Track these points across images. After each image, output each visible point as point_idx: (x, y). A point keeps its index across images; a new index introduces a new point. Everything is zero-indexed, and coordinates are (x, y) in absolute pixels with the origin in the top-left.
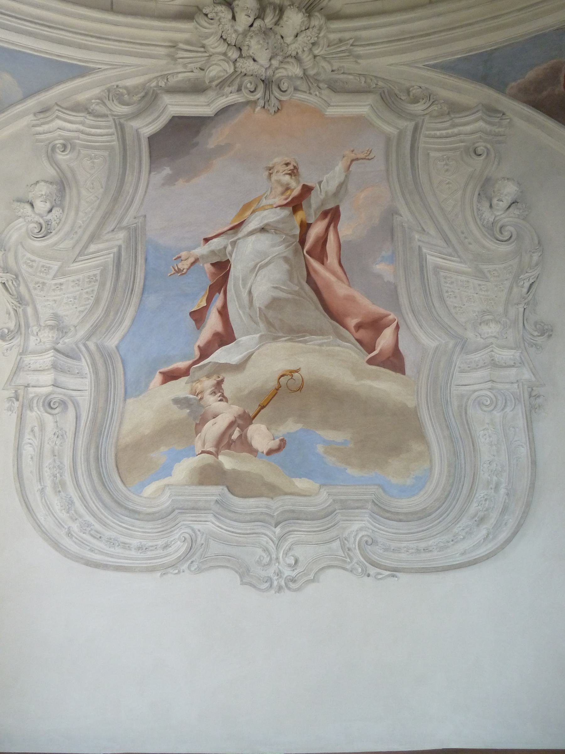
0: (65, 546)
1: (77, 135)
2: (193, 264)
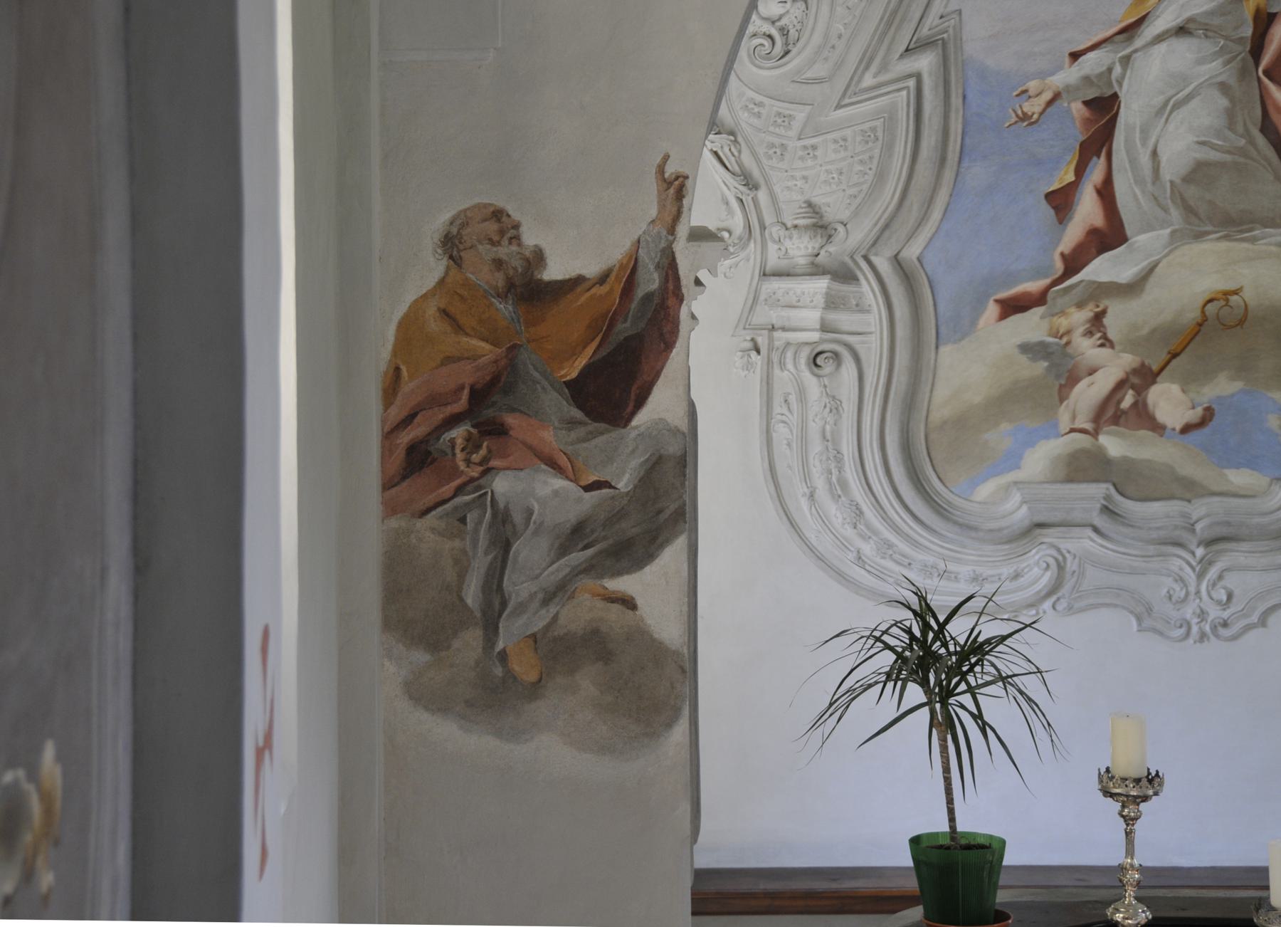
0: (851, 577)
2: (1050, 103)
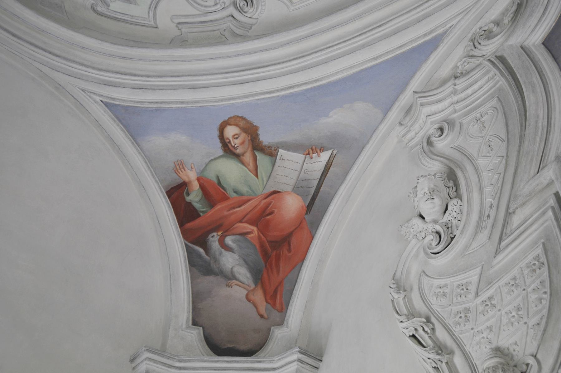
1: (452, 109)
